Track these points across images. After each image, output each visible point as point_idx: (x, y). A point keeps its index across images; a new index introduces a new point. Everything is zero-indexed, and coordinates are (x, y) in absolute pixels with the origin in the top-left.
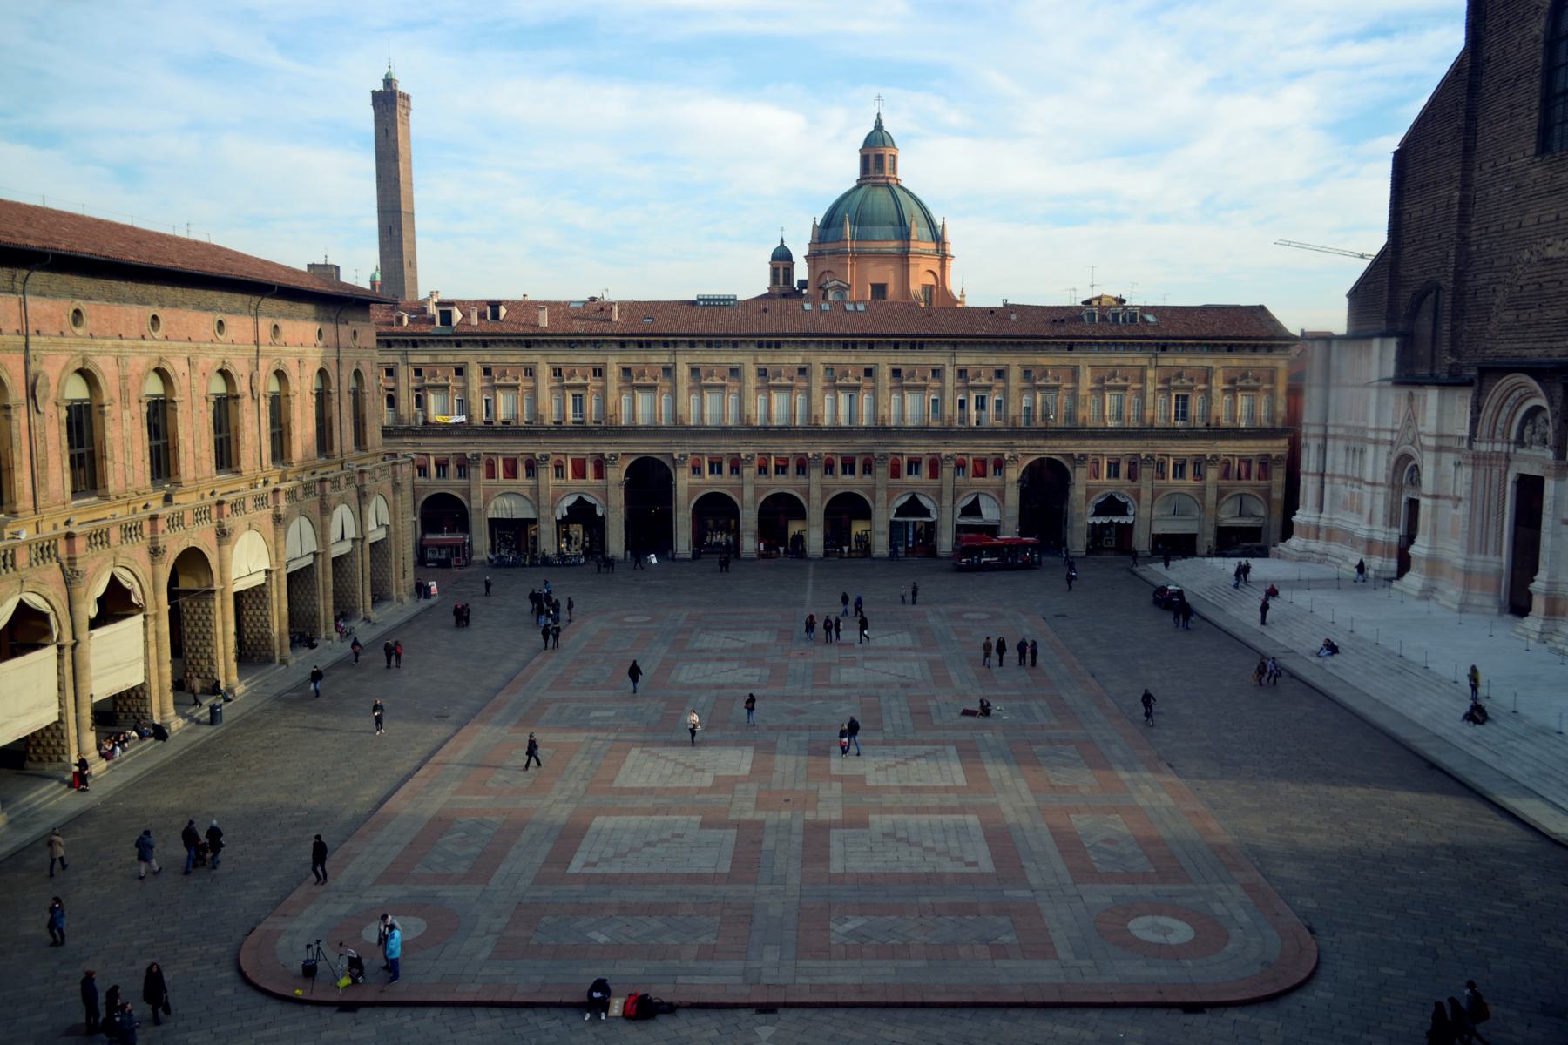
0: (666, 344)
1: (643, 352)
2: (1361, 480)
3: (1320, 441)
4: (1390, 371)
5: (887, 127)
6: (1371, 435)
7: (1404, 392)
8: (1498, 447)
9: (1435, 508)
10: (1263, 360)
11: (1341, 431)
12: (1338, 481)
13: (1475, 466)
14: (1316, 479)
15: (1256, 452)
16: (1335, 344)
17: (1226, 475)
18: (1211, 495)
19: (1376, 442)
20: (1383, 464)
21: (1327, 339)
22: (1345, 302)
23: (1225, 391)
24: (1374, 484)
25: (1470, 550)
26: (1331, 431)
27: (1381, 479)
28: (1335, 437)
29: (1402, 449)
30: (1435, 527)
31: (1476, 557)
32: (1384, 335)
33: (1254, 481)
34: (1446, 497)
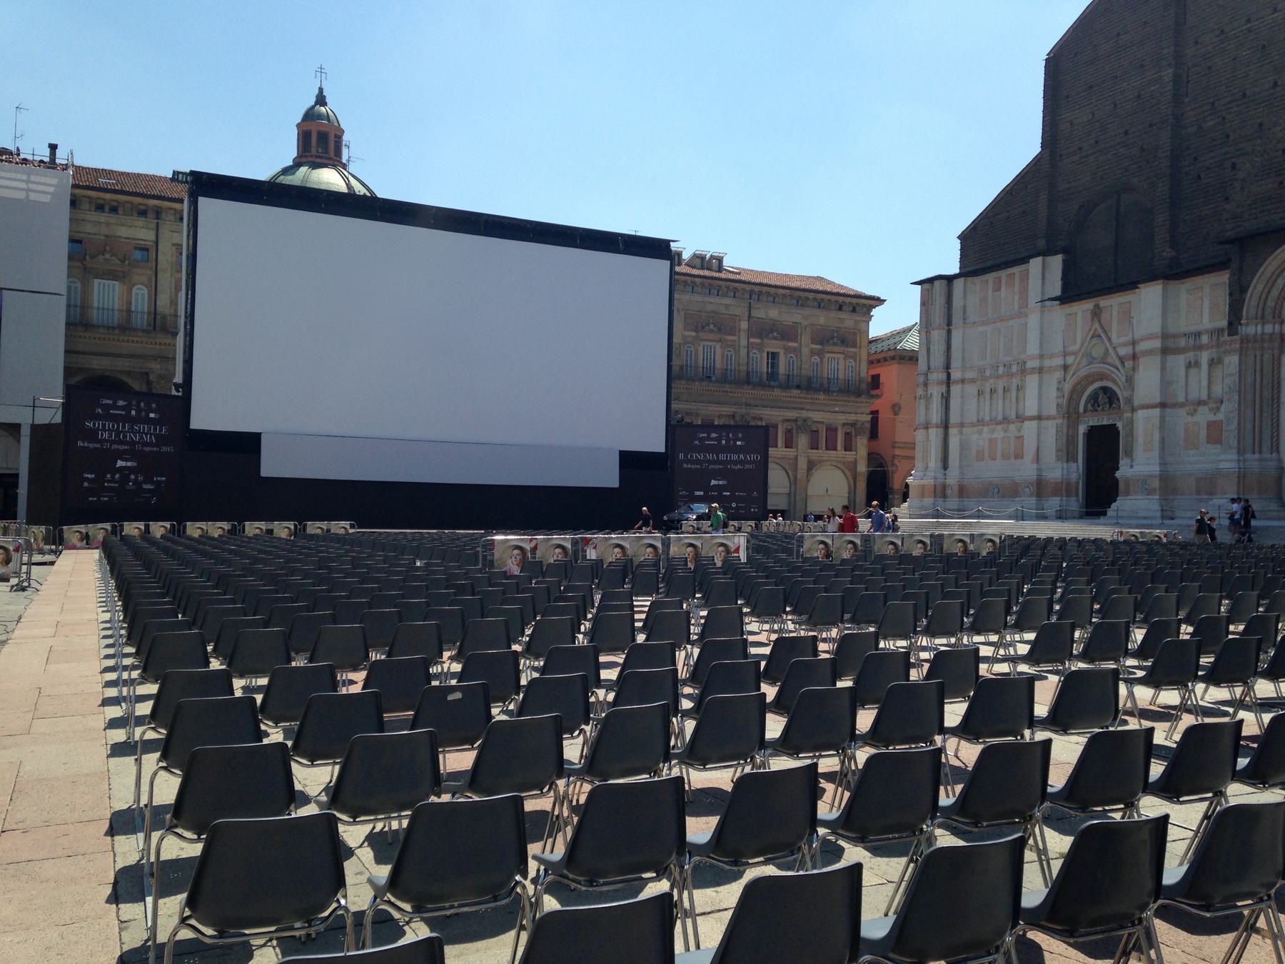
0: (143, 213)
1: (103, 217)
2: (1021, 418)
3: (944, 388)
4: (1057, 291)
5: (335, 105)
6: (1030, 364)
7: (1082, 309)
8: (1269, 329)
9: (1162, 418)
10: (848, 320)
11: (970, 375)
12: (966, 430)
13: (1242, 352)
14: (941, 431)
15: (842, 418)
16: (958, 284)
17: (814, 446)
18: (802, 465)
19: (1041, 370)
20: (1052, 393)
21: (949, 279)
22: (957, 245)
23: (813, 353)
24: (1039, 418)
25: (1240, 451)
26: (956, 375)
27: (1053, 412)
28: (963, 381)
29: (1083, 373)
30: (1163, 441)
31: (1249, 456)
32: (1046, 253)
33: (840, 451)
34: (1175, 405)
